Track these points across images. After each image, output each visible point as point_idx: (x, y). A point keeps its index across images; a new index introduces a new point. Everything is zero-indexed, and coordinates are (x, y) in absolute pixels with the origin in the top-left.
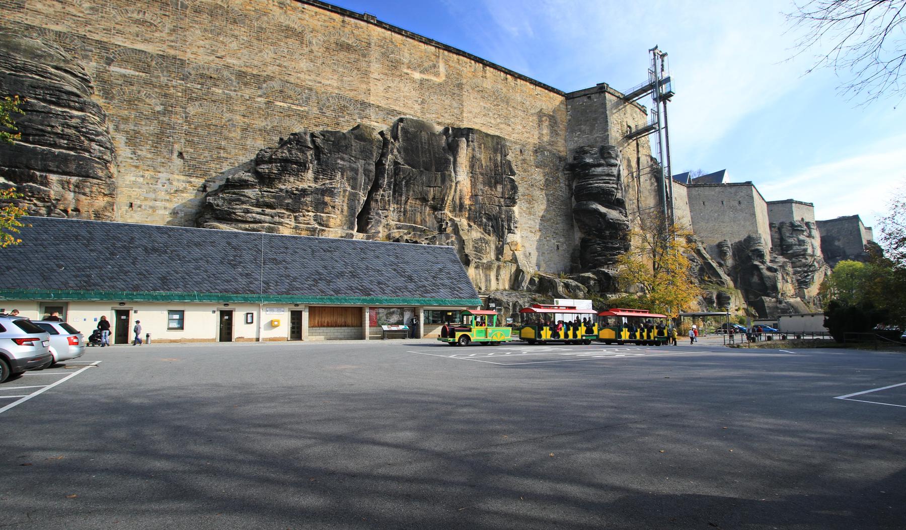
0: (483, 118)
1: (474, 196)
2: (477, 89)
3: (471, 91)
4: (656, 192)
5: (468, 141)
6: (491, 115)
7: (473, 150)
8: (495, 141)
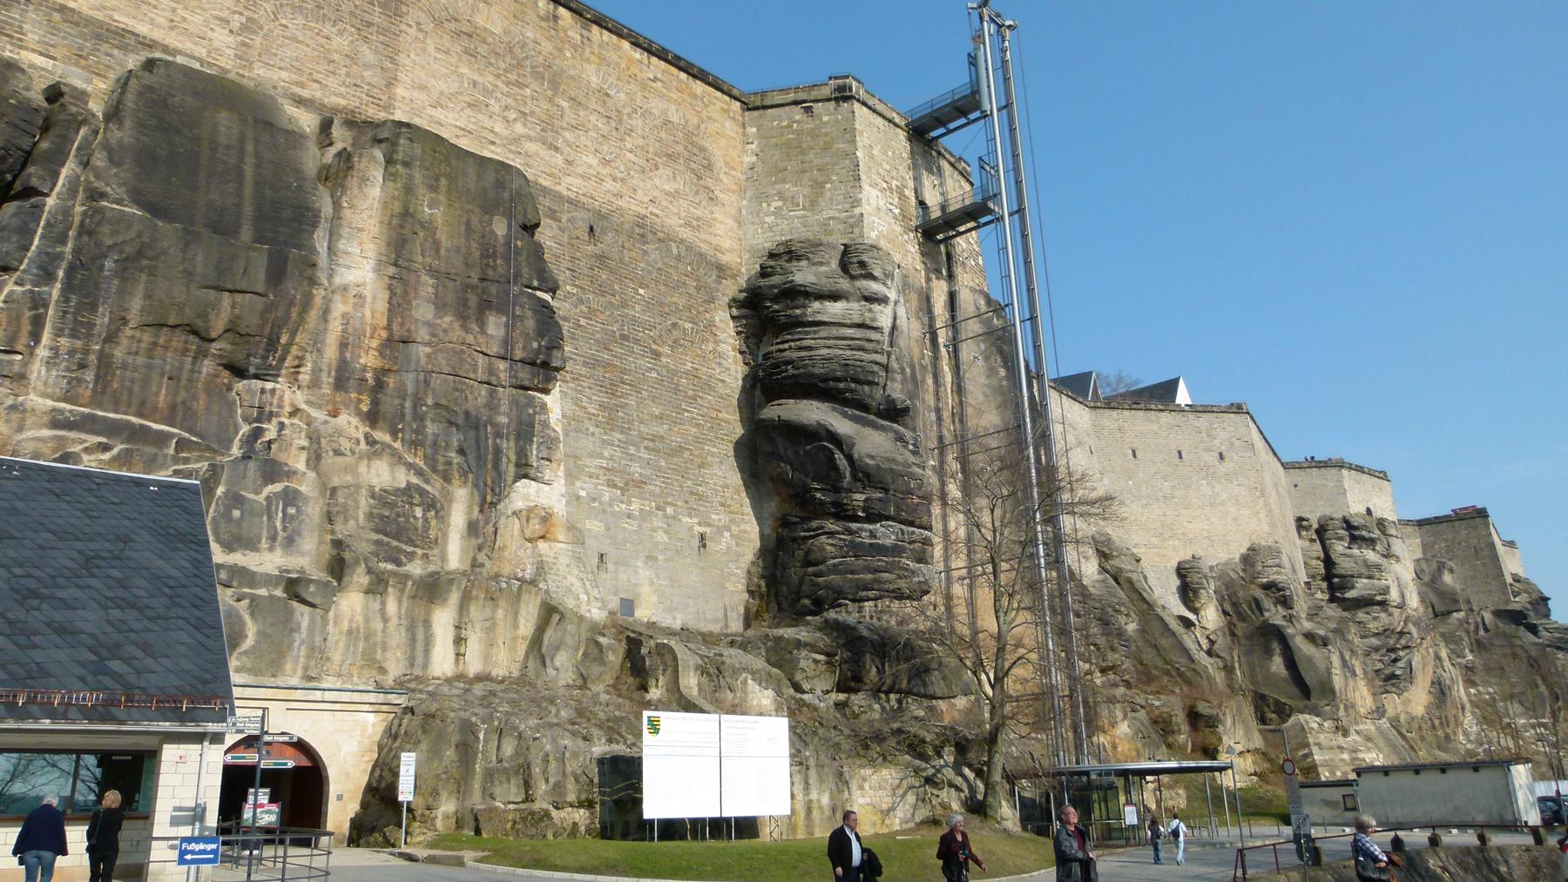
0: (468, 111)
1: (396, 343)
2: (453, 26)
3: (429, 27)
4: (1004, 394)
5: (389, 161)
6: (495, 107)
7: (409, 190)
8: (490, 177)
